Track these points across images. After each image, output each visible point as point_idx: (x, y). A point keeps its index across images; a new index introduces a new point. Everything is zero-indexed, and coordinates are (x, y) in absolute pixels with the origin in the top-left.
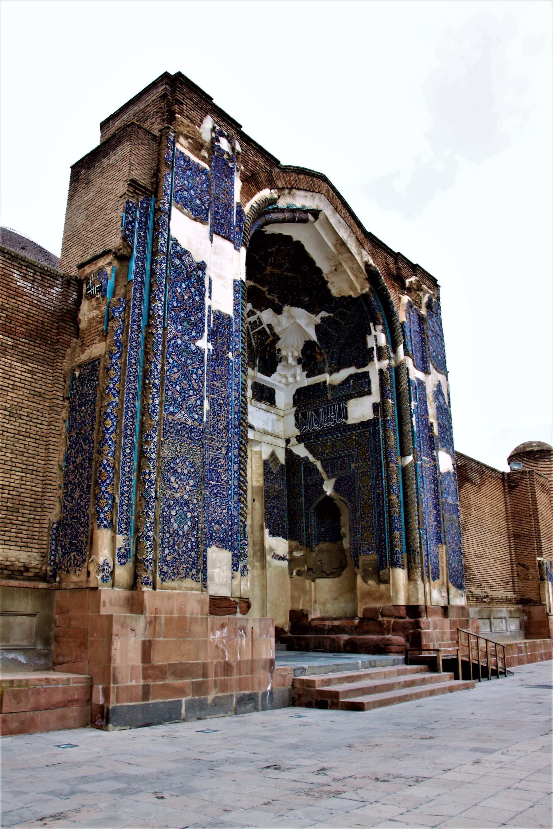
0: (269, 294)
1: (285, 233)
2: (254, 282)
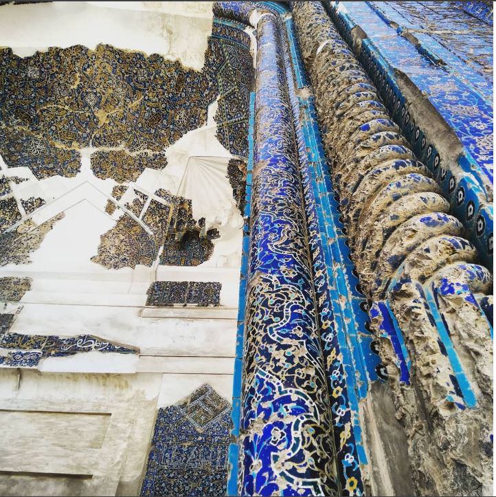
0: (131, 151)
1: (64, 44)
2: (94, 145)
